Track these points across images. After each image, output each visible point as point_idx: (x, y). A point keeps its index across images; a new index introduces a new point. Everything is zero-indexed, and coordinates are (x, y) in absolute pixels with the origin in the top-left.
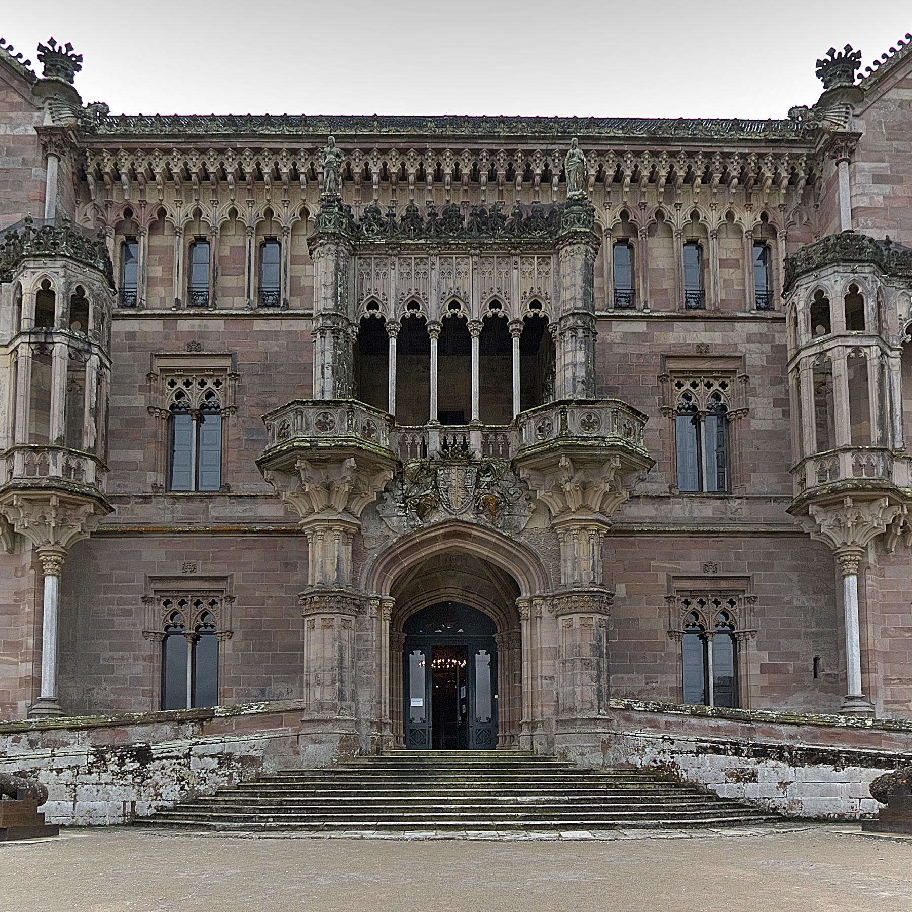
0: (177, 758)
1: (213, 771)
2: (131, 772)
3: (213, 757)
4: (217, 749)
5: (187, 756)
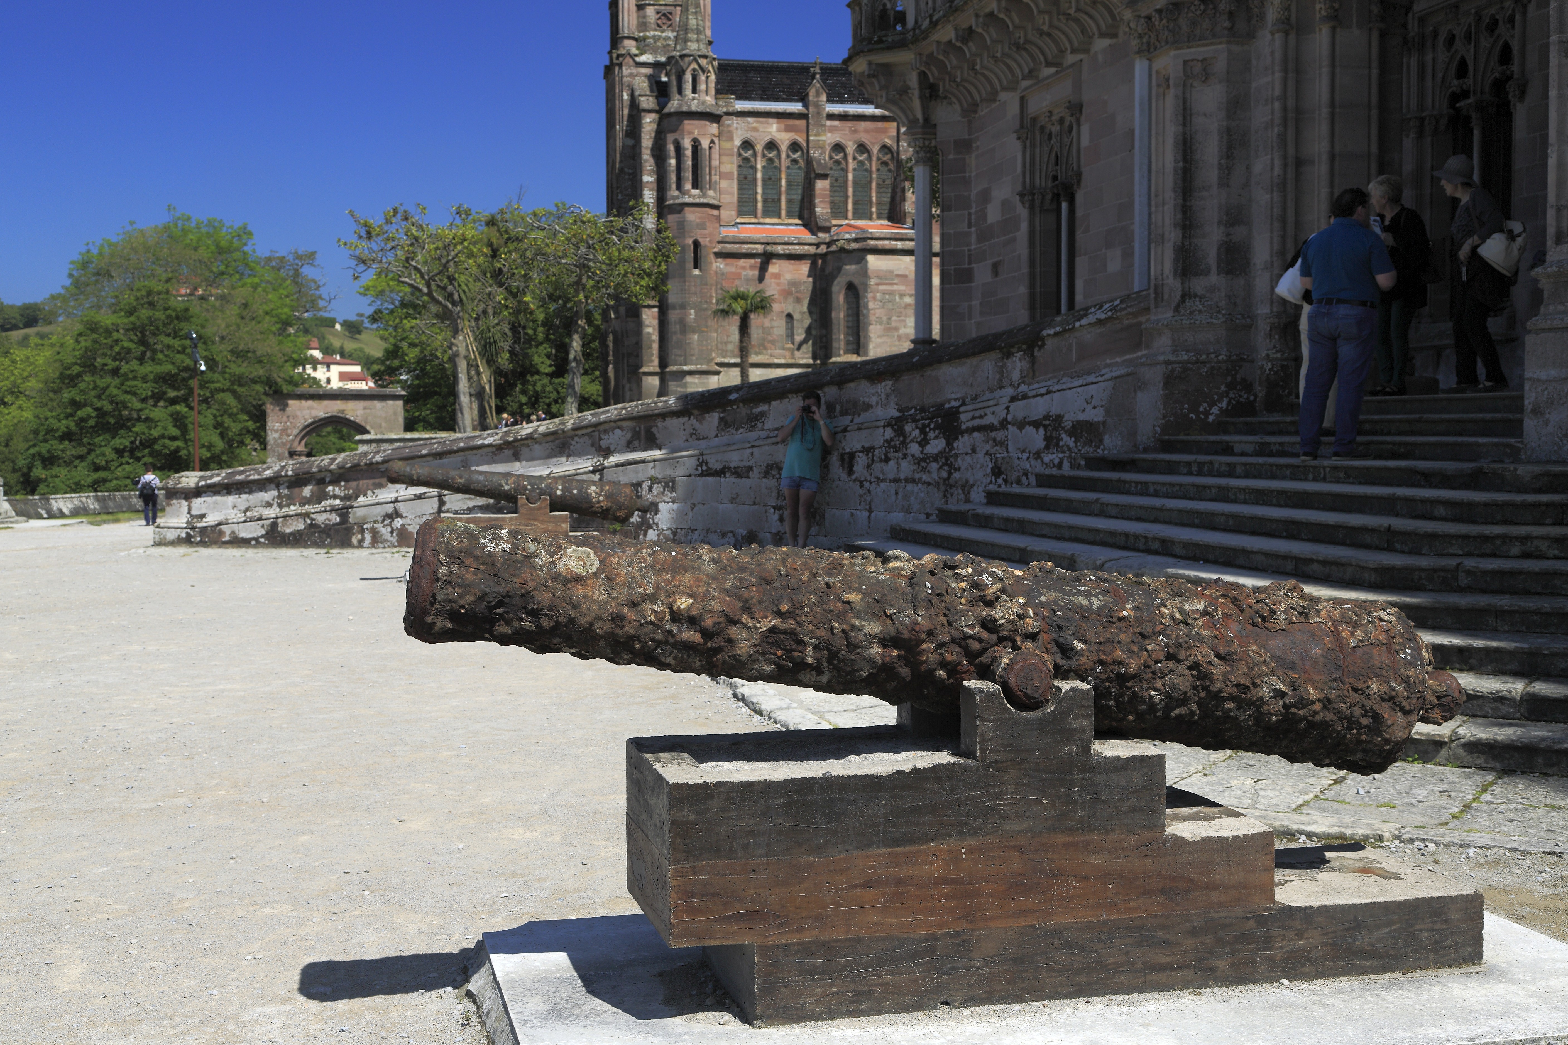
0: (991, 428)
1: (1038, 455)
2: (935, 458)
3: (1036, 424)
4: (1039, 407)
5: (1004, 424)
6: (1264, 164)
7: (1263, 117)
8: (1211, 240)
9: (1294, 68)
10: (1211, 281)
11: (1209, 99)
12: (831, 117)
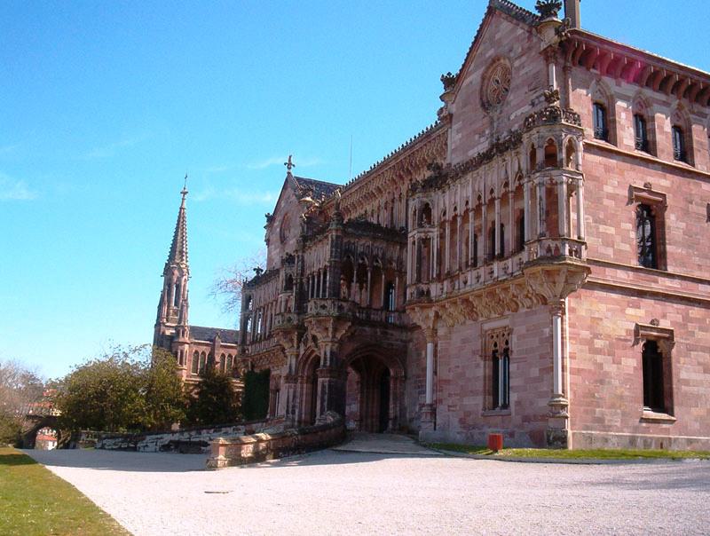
6: (298, 400)
7: (298, 394)
8: (290, 410)
9: (302, 388)
10: (290, 415)
11: (291, 391)
12: (222, 346)
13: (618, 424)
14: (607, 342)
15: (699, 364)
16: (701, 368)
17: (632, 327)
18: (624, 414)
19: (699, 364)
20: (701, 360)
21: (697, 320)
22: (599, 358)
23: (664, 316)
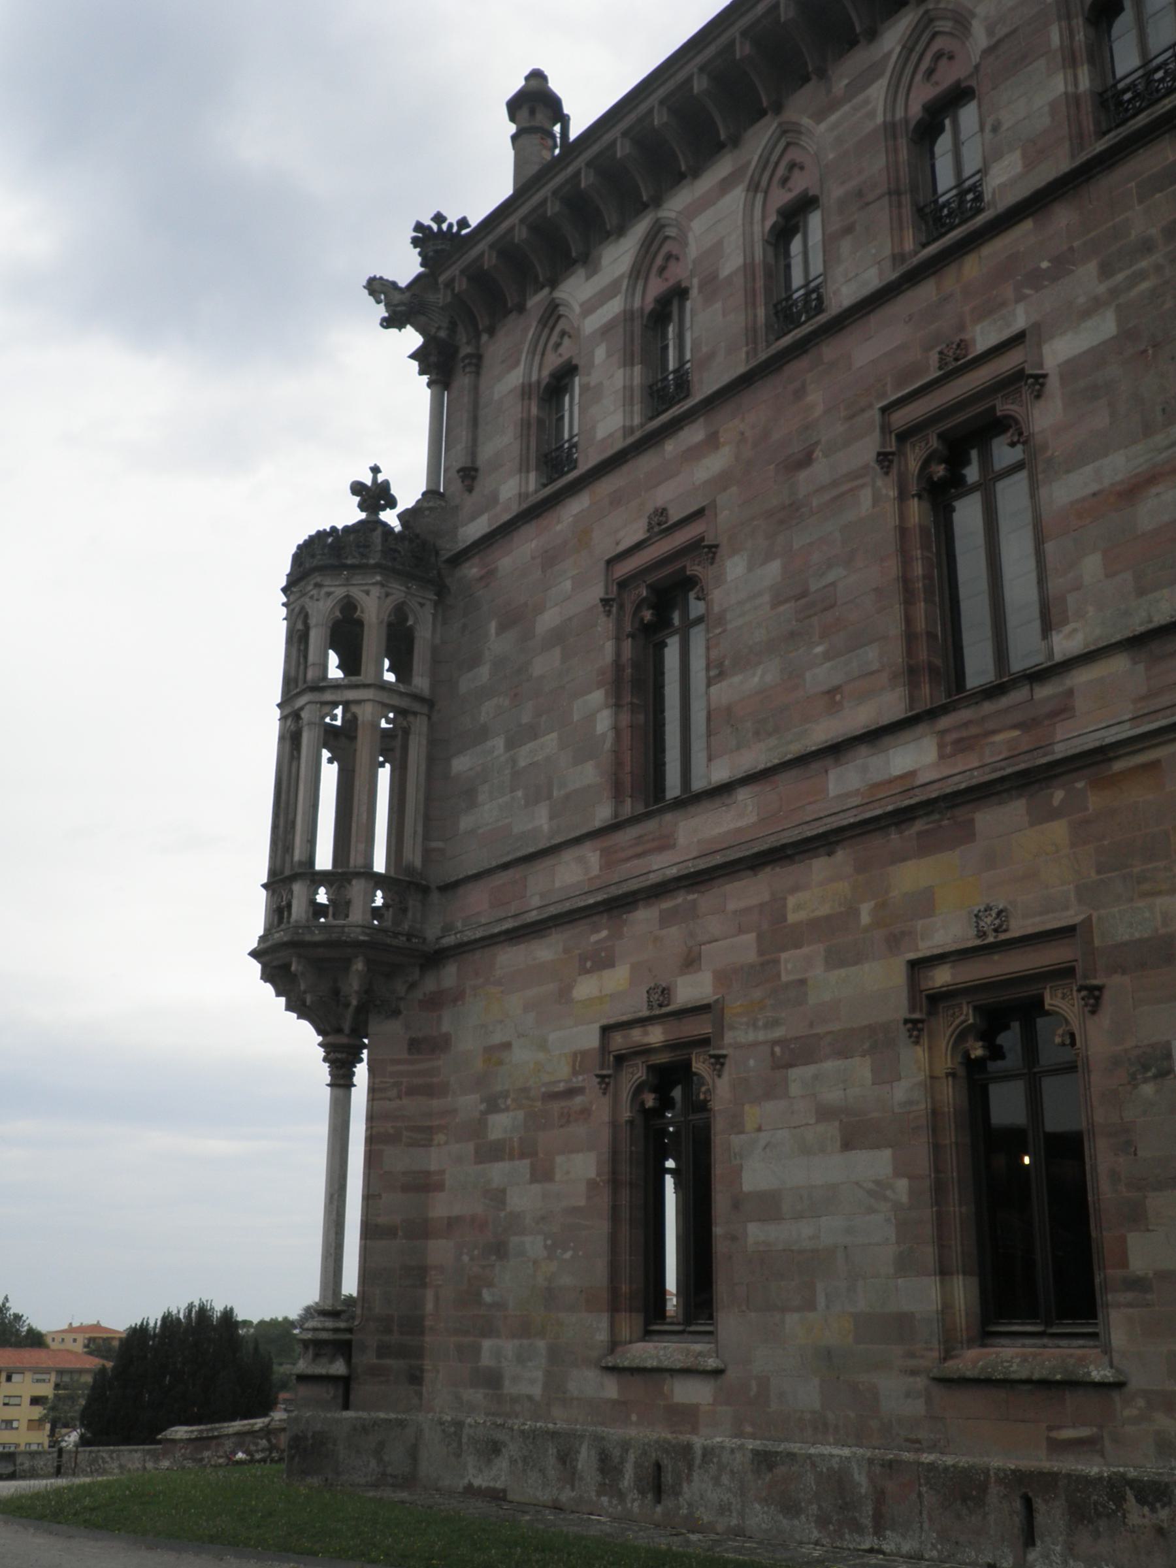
13: (537, 1391)
14: (520, 1114)
15: (825, 1113)
16: (831, 1130)
17: (590, 1039)
18: (555, 1355)
19: (825, 1113)
20: (832, 1096)
21: (819, 927)
22: (498, 1172)
23: (691, 962)
